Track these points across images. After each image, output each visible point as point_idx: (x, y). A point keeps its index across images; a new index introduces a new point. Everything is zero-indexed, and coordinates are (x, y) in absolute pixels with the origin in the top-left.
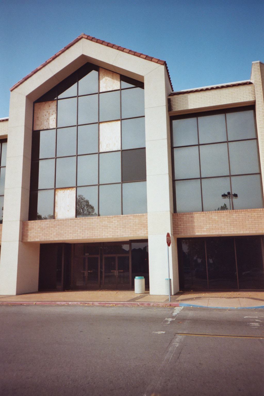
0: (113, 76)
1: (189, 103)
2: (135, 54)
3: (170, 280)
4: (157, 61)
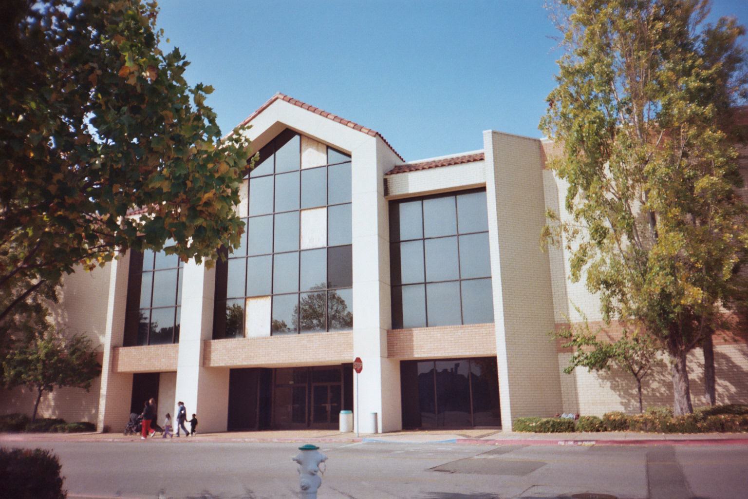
0: (317, 146)
1: (409, 185)
2: (341, 121)
3: (376, 414)
4: (367, 131)
